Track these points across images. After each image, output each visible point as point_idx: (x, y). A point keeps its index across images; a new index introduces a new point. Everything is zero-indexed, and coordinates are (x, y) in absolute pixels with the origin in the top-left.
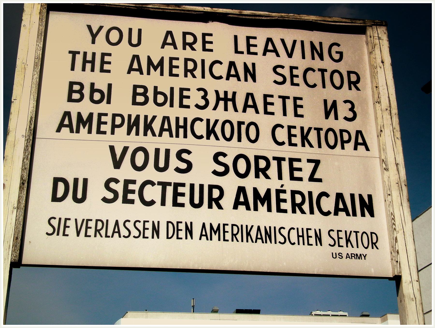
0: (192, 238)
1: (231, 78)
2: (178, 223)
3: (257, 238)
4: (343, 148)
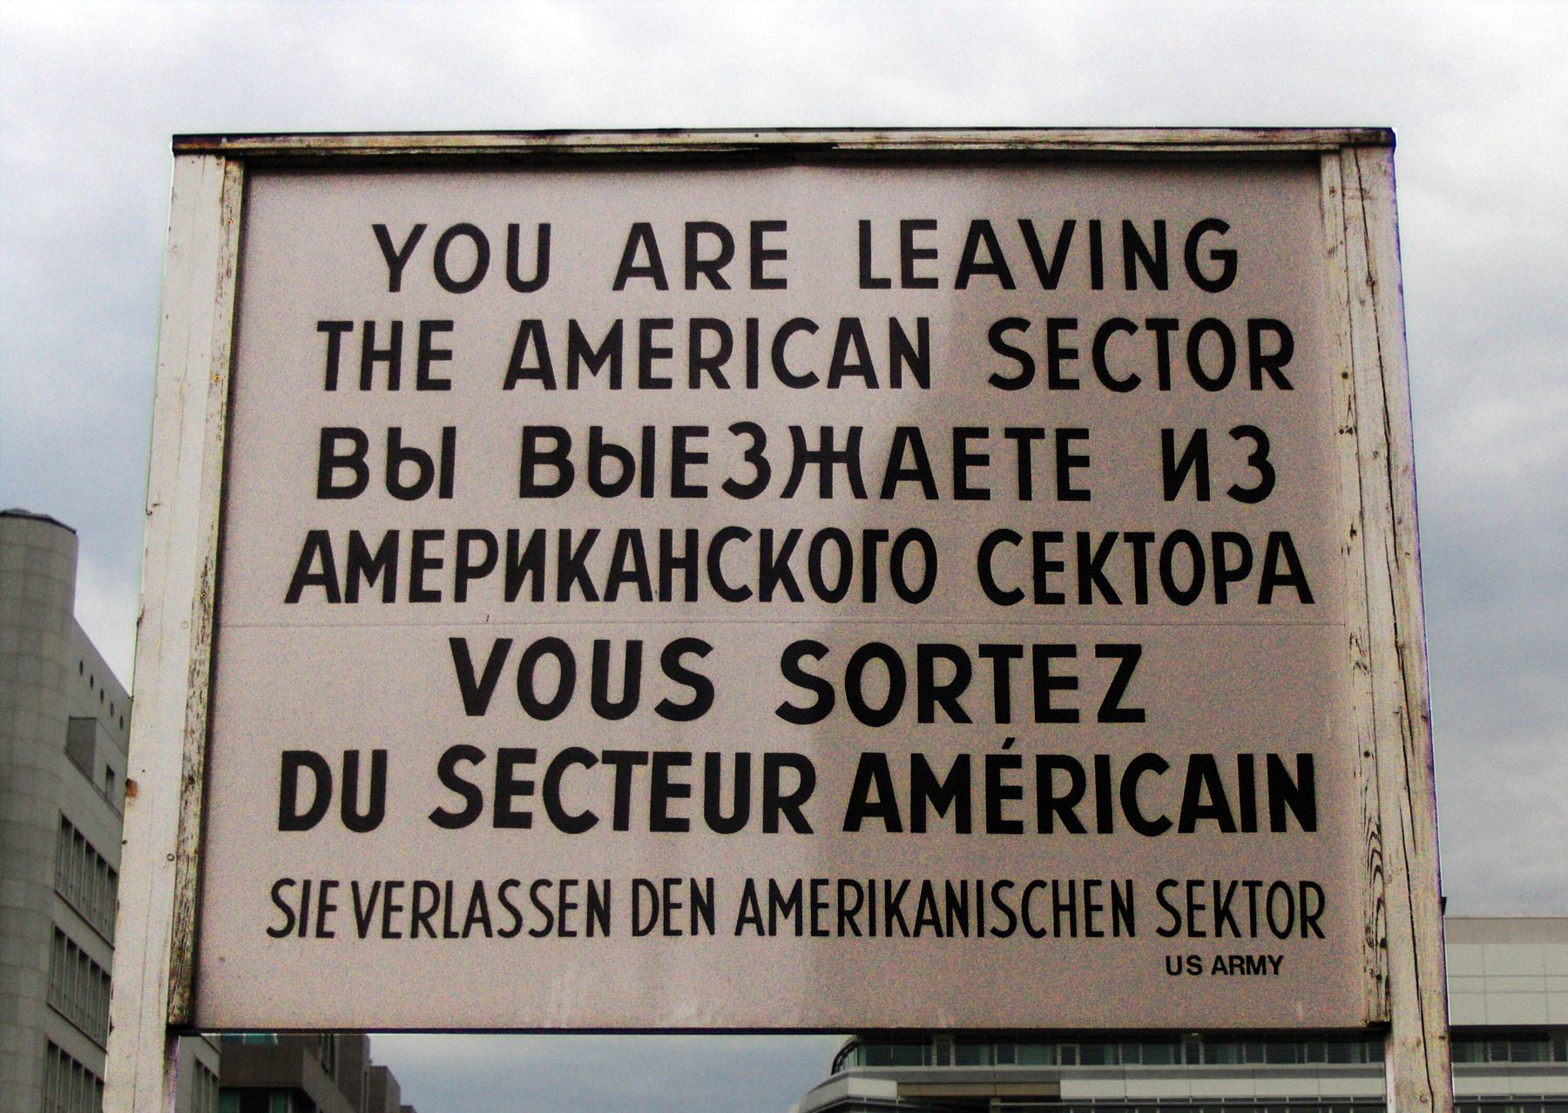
0: (712, 932)
1: (845, 379)
2: (668, 883)
3: (920, 922)
4: (1221, 598)
